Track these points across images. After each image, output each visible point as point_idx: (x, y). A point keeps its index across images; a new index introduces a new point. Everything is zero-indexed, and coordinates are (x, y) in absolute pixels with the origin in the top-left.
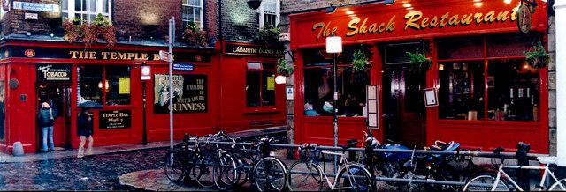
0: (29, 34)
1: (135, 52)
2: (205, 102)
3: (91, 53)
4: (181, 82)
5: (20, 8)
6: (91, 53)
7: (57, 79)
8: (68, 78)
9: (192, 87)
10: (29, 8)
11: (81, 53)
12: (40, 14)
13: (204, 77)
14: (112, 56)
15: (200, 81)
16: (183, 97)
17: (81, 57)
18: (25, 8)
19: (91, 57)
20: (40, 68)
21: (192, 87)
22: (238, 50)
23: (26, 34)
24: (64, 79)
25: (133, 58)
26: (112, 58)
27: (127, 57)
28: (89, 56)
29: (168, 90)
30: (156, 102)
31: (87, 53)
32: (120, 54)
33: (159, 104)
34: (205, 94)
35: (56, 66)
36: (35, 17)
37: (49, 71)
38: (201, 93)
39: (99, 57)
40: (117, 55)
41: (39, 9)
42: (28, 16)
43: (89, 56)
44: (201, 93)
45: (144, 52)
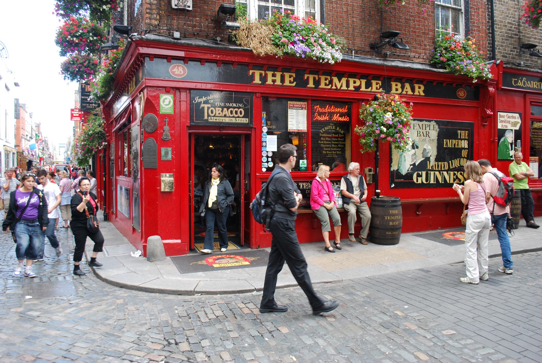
0: (177, 35)
1: (361, 76)
3: (287, 75)
4: (434, 134)
7: (227, 120)
8: (245, 121)
9: (449, 143)
11: (270, 74)
15: (463, 134)
16: (438, 159)
17: (269, 82)
19: (287, 83)
21: (449, 143)
22: (520, 84)
25: (358, 88)
26: (322, 86)
27: (348, 85)
28: (283, 80)
29: (414, 146)
30: (394, 168)
31: (279, 74)
32: (335, 80)
33: (397, 173)
38: (464, 153)
39: (301, 82)
40: (331, 82)
43: (283, 80)
45: (376, 78)
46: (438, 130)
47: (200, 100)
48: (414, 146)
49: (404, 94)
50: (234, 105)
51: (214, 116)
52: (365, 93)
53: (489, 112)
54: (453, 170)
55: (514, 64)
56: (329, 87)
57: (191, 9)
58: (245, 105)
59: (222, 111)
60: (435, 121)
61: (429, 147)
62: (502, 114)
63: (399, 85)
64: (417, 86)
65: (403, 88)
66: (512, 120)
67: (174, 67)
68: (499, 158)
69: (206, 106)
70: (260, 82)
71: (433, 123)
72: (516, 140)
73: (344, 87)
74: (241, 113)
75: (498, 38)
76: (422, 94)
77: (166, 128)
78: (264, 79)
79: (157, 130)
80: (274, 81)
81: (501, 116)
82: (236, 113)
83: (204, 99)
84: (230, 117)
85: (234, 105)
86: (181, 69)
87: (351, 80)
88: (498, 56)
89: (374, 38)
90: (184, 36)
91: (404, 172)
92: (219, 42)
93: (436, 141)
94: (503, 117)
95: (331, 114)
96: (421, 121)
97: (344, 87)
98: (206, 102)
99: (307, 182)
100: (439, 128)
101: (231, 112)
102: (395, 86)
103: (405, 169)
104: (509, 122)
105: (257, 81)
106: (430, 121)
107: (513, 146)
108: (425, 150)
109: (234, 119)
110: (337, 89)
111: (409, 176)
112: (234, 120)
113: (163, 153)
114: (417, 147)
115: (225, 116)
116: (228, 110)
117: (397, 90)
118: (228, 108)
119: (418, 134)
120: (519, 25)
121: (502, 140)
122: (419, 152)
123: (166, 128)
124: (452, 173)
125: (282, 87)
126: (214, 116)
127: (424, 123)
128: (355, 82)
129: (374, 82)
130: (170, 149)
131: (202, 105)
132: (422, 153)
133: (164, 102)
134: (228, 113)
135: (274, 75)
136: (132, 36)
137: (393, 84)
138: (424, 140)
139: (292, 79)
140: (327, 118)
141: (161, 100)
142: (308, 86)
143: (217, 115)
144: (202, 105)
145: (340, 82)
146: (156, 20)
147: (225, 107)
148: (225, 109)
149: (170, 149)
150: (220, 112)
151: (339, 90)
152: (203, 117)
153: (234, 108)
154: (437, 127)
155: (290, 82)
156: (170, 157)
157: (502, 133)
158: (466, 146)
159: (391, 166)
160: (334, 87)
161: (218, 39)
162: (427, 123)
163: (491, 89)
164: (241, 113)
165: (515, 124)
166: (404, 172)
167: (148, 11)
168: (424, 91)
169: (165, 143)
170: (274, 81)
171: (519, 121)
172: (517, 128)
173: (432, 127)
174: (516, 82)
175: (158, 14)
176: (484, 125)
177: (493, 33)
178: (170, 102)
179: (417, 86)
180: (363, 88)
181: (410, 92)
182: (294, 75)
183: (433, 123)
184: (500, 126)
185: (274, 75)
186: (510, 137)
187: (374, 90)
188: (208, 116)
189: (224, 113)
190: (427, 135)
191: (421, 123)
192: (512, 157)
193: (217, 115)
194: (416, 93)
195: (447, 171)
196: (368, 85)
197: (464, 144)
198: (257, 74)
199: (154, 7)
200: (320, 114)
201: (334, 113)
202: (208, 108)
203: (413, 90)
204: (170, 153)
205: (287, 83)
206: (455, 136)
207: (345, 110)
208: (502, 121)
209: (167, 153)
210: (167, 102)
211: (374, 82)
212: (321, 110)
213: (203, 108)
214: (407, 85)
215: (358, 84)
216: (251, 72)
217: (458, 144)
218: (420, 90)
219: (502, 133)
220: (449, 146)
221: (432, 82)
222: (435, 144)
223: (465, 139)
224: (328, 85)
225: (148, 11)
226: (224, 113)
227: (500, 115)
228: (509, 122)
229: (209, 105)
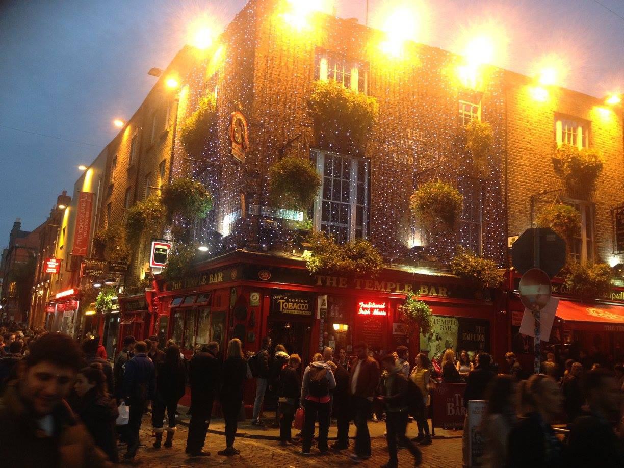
4: (455, 328)
6: (341, 280)
7: (296, 312)
8: (309, 313)
11: (329, 278)
17: (328, 284)
19: (341, 285)
23: (261, 249)
24: (304, 313)
26: (367, 288)
28: (338, 283)
29: (438, 338)
31: (335, 279)
37: (287, 301)
43: (338, 283)
46: (458, 325)
48: (438, 338)
49: (430, 295)
50: (302, 301)
51: (287, 309)
56: (372, 289)
59: (293, 305)
60: (456, 318)
69: (282, 301)
70: (321, 284)
71: (454, 319)
80: (331, 284)
84: (298, 310)
85: (302, 301)
86: (266, 274)
92: (294, 254)
93: (456, 334)
95: (372, 310)
96: (444, 317)
98: (281, 299)
100: (459, 323)
101: (300, 307)
107: (527, 341)
108: (447, 341)
112: (301, 313)
114: (441, 339)
115: (295, 309)
116: (297, 304)
118: (297, 303)
126: (287, 309)
127: (447, 319)
128: (391, 285)
131: (279, 301)
132: (445, 344)
133: (253, 297)
135: (331, 280)
141: (251, 296)
142: (356, 288)
143: (289, 308)
144: (279, 301)
145: (380, 285)
147: (295, 302)
148: (295, 304)
150: (291, 306)
151: (379, 291)
152: (279, 309)
153: (301, 303)
154: (457, 323)
155: (343, 285)
158: (484, 340)
162: (449, 319)
164: (306, 307)
170: (331, 284)
173: (453, 323)
178: (257, 298)
183: (454, 319)
185: (331, 280)
188: (283, 308)
189: (294, 307)
191: (443, 319)
192: (526, 350)
193: (289, 308)
197: (481, 338)
200: (364, 309)
202: (283, 303)
207: (383, 306)
212: (366, 306)
213: (280, 302)
214: (433, 290)
217: (476, 338)
220: (468, 338)
222: (456, 337)
223: (482, 334)
224: (371, 287)
226: (294, 307)
227: (514, 314)
229: (284, 301)
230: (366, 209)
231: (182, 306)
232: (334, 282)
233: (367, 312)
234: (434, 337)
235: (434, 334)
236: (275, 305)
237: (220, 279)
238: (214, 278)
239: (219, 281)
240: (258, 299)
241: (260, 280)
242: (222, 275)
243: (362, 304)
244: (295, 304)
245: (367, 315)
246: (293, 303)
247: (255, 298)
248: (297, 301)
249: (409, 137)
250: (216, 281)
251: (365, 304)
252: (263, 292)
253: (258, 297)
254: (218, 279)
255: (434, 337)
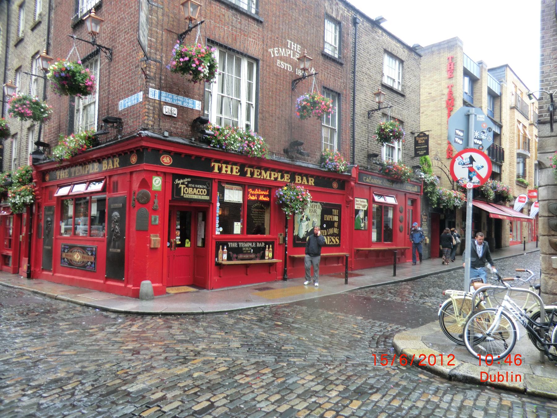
2: (338, 235)
3: (234, 167)
4: (319, 211)
5: (157, 98)
7: (195, 197)
8: (207, 198)
9: (328, 218)
10: (169, 100)
11: (224, 166)
12: (181, 109)
13: (338, 207)
14: (256, 173)
15: (335, 212)
17: (224, 172)
18: (163, 99)
19: (234, 173)
20: (177, 181)
21: (328, 218)
22: (368, 181)
25: (276, 179)
26: (255, 176)
27: (270, 177)
28: (232, 171)
30: (296, 233)
31: (229, 167)
32: (263, 172)
33: (297, 238)
34: (339, 227)
35: (195, 181)
36: (175, 111)
37: (187, 186)
38: (336, 225)
39: (243, 173)
40: (260, 174)
41: (180, 103)
42: (166, 110)
43: (232, 171)
44: (336, 225)
45: (287, 172)
47: (179, 182)
52: (280, 182)
53: (351, 198)
54: (329, 235)
55: (364, 167)
56: (259, 177)
57: (176, 116)
58: (208, 187)
60: (321, 203)
61: (316, 220)
62: (357, 199)
63: (300, 178)
64: (310, 179)
65: (302, 179)
66: (363, 204)
67: (163, 158)
68: (355, 228)
69: (183, 186)
71: (319, 204)
72: (365, 217)
73: (268, 178)
74: (205, 192)
75: (356, 150)
76: (313, 184)
77: (156, 201)
78: (220, 169)
79: (149, 202)
80: (226, 171)
81: (357, 201)
82: (202, 192)
83: (181, 181)
85: (201, 186)
86: (168, 159)
87: (273, 173)
88: (356, 162)
89: (287, 145)
90: (171, 135)
91: (301, 236)
94: (358, 201)
95: (258, 195)
97: (268, 178)
98: (183, 184)
99: (244, 242)
102: (298, 179)
103: (302, 234)
104: (361, 205)
105: (216, 170)
106: (317, 202)
108: (313, 222)
109: (200, 196)
110: (264, 179)
111: (304, 239)
112: (200, 197)
113: (153, 219)
114: (309, 220)
115: (195, 194)
117: (299, 181)
118: (197, 188)
119: (310, 211)
120: (368, 142)
121: (357, 216)
122: (310, 223)
123: (156, 201)
124: (329, 237)
125: (231, 175)
128: (274, 175)
129: (286, 175)
130: (157, 216)
131: (180, 186)
134: (197, 192)
136: (141, 133)
137: (297, 177)
138: (313, 215)
139: (237, 170)
140: (256, 198)
141: (154, 180)
145: (266, 173)
146: (152, 121)
148: (195, 189)
149: (157, 216)
153: (200, 188)
156: (157, 222)
157: (357, 212)
158: (337, 220)
159: (294, 232)
160: (262, 178)
161: (193, 139)
163: (352, 183)
164: (205, 192)
165: (364, 206)
166: (301, 236)
167: (147, 114)
168: (314, 183)
169: (155, 211)
170: (226, 171)
171: (367, 204)
172: (366, 209)
174: (366, 179)
175: (153, 117)
176: (347, 207)
177: (354, 146)
179: (310, 179)
180: (279, 179)
181: (306, 183)
182: (239, 168)
184: (356, 208)
185: (226, 167)
186: (361, 215)
187: (286, 180)
188: (184, 193)
190: (315, 212)
194: (310, 184)
195: (326, 236)
196: (282, 177)
197: (336, 218)
198: (216, 165)
199: (151, 112)
200: (252, 195)
201: (260, 195)
202: (184, 188)
203: (308, 182)
204: (158, 219)
205: (234, 173)
206: (331, 213)
208: (357, 204)
209: (155, 220)
210: (157, 182)
211: (286, 175)
212: (253, 192)
213: (181, 188)
214: (305, 178)
215: (276, 176)
216: (213, 164)
218: (312, 182)
219: (357, 212)
220: (328, 219)
221: (318, 177)
222: (320, 218)
225: (147, 114)
228: (361, 205)
230: (254, 106)
231: (70, 194)
232: (229, 169)
233: (253, 198)
234: (305, 219)
235: (305, 216)
236: (176, 190)
237: (117, 164)
238: (108, 164)
239: (115, 167)
240: (160, 183)
241: (161, 164)
242: (118, 161)
243: (250, 190)
244: (195, 189)
245: (255, 200)
246: (193, 188)
247: (157, 182)
248: (196, 186)
249: (289, 46)
250: (112, 167)
251: (253, 190)
252: (164, 175)
253: (161, 181)
254: (113, 166)
255: (305, 219)
